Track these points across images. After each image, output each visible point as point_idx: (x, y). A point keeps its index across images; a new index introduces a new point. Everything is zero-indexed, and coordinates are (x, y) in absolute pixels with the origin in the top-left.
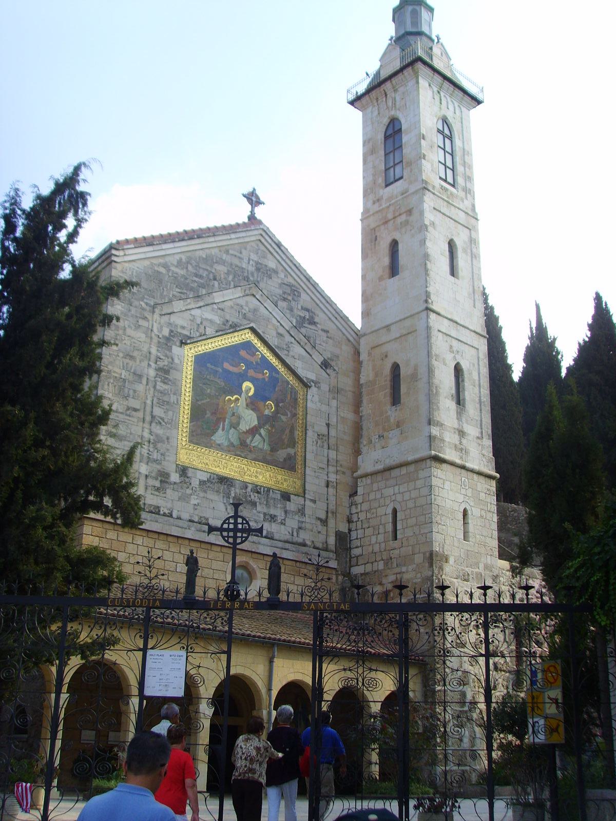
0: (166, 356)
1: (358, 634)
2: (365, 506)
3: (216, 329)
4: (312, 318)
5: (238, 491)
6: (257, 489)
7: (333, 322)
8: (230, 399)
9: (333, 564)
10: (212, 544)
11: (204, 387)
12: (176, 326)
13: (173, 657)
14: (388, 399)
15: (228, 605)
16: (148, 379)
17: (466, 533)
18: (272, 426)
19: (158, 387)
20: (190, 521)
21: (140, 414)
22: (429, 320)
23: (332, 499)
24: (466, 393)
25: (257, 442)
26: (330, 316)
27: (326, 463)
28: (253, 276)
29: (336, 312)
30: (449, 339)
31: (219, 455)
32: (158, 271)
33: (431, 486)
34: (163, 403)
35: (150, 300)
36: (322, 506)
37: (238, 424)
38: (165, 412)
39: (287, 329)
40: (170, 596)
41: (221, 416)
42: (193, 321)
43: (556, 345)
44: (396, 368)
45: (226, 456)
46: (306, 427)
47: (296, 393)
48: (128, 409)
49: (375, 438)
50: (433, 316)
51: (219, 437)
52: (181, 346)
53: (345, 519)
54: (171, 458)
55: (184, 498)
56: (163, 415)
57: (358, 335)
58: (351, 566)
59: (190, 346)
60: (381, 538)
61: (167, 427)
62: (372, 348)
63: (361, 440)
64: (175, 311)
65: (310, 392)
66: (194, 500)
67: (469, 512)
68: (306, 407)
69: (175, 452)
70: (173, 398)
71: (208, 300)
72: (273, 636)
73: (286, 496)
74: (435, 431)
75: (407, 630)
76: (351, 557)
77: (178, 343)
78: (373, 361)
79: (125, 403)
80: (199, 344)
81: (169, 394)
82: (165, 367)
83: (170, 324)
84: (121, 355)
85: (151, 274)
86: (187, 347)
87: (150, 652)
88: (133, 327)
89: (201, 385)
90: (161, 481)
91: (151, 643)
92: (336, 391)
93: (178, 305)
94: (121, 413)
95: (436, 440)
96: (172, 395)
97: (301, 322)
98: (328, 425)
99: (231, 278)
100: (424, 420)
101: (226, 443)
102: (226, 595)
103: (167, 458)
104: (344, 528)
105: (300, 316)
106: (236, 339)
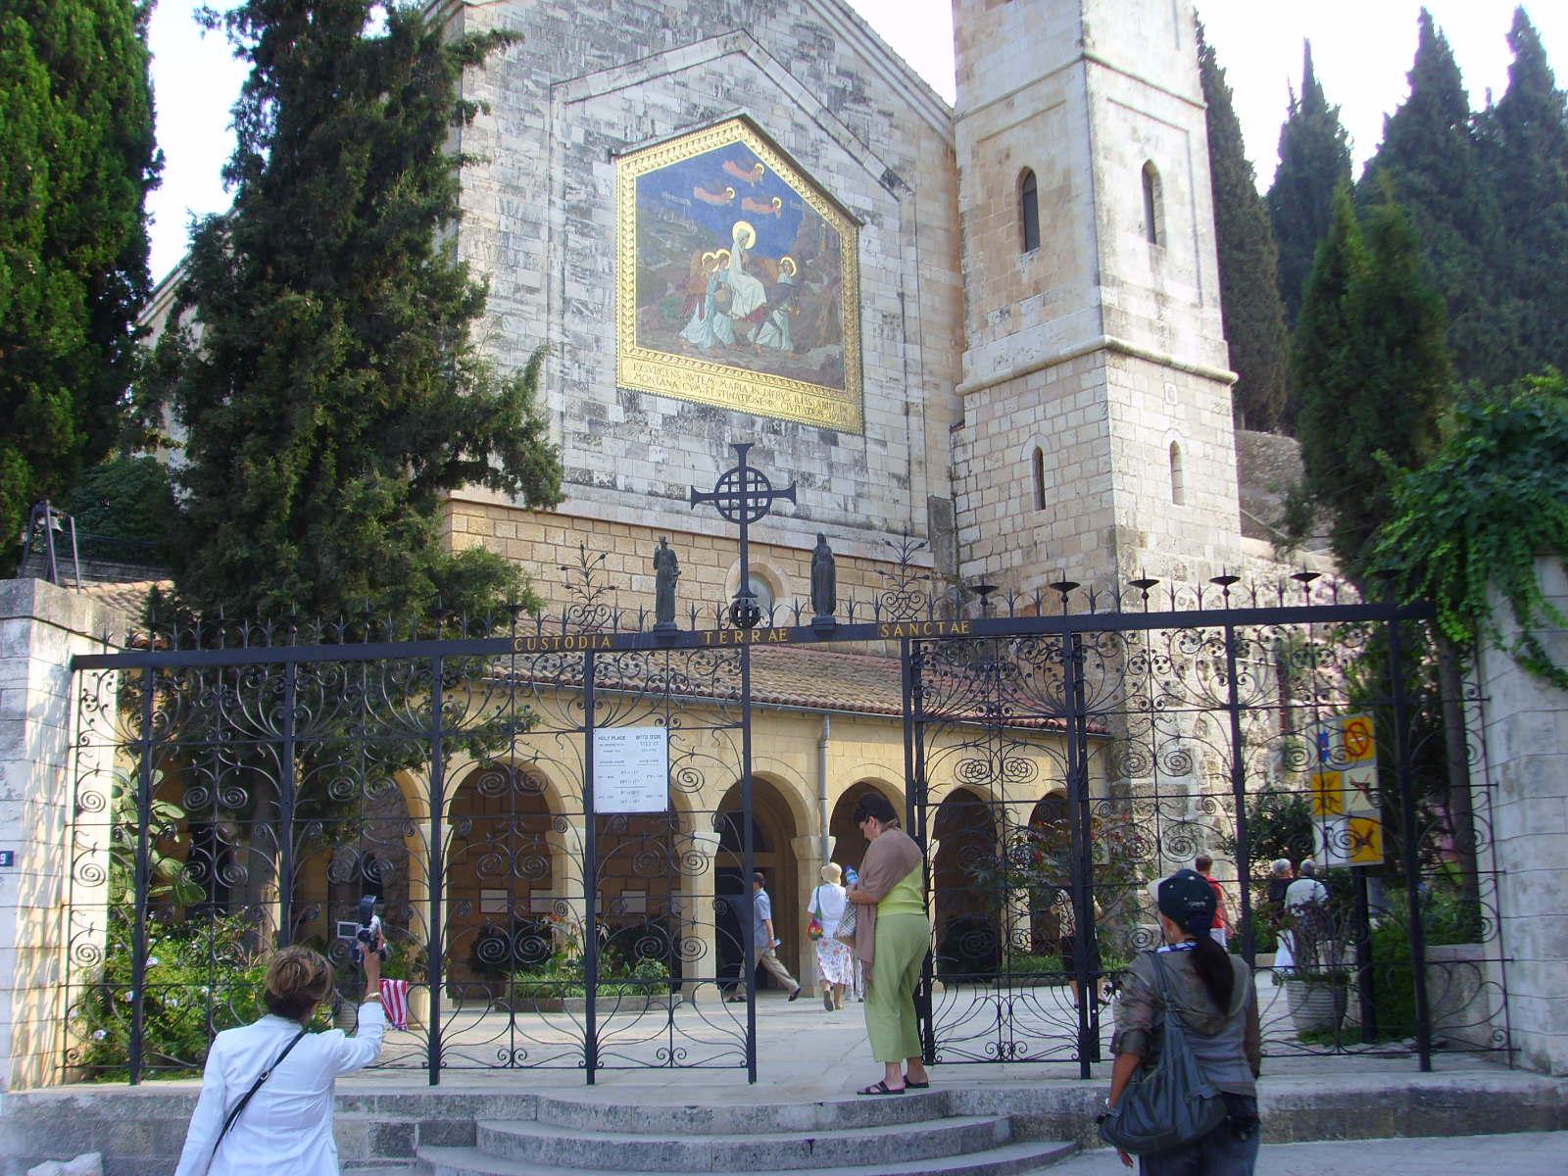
0: (582, 182)
1: (988, 677)
2: (981, 448)
3: (675, 123)
4: (860, 90)
5: (737, 431)
6: (773, 427)
7: (901, 96)
8: (712, 259)
9: (924, 559)
10: (694, 535)
11: (659, 237)
12: (597, 123)
13: (642, 740)
14: (1016, 239)
15: (739, 637)
16: (550, 229)
17: (1177, 489)
18: (795, 304)
19: (571, 244)
20: (651, 494)
21: (542, 298)
22: (1089, 80)
23: (917, 437)
24: (1168, 220)
25: (767, 336)
26: (895, 84)
28: (739, 15)
29: (906, 76)
30: (1130, 115)
32: (553, 18)
33: (1106, 402)
34: (582, 274)
35: (544, 76)
36: (898, 450)
37: (731, 304)
39: (812, 114)
40: (628, 621)
42: (628, 111)
43: (1340, 119)
44: (1027, 178)
47: (836, 238)
48: (518, 289)
49: (992, 317)
50: (1095, 71)
51: (695, 331)
53: (945, 474)
54: (607, 377)
55: (636, 452)
56: (584, 297)
57: (951, 118)
58: (959, 563)
59: (628, 159)
60: (1014, 506)
62: (981, 141)
63: (966, 322)
66: (655, 455)
67: (1182, 450)
70: (602, 263)
71: (655, 68)
72: (821, 700)
73: (829, 437)
74: (1108, 296)
75: (1079, 666)
76: (959, 546)
77: (603, 156)
78: (983, 166)
79: (512, 278)
80: (644, 154)
82: (582, 204)
83: (586, 120)
84: (496, 186)
85: (541, 24)
86: (621, 163)
87: (598, 733)
88: (515, 132)
90: (590, 423)
91: (598, 719)
92: (913, 230)
93: (597, 82)
94: (506, 298)
95: (1113, 315)
96: (599, 258)
97: (839, 98)
98: (901, 296)
99: (696, 20)
100: (1089, 278)
101: (709, 343)
102: (733, 619)
103: (598, 379)
104: (942, 490)
105: (836, 88)
106: (715, 140)
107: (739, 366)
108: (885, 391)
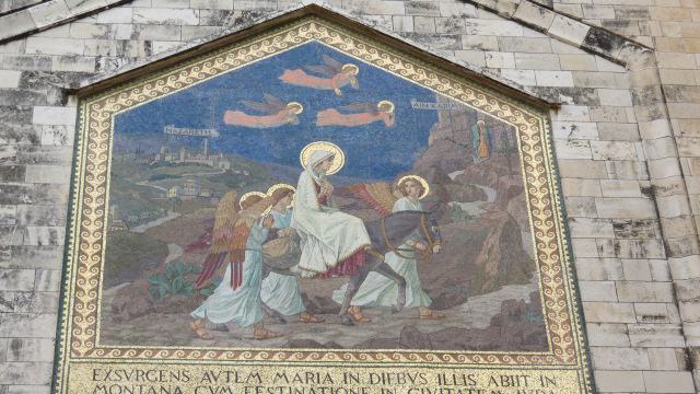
0: (12, 135)
8: (259, 199)
11: (156, 185)
12: (48, 60)
18: (430, 239)
25: (374, 288)
27: (669, 298)
31: (224, 356)
37: (296, 256)
38: (5, 276)
41: (225, 249)
42: (105, 37)
45: (255, 353)
46: (564, 211)
47: (508, 134)
51: (224, 304)
52: (64, 103)
61: (15, 315)
64: (39, 26)
65: (558, 120)
68: (555, 163)
69: (46, 376)
70: (36, 235)
77: (54, 97)
81: (24, 227)
82: (7, 164)
89: (143, 184)
96: (31, 229)
98: (650, 192)
101: (251, 320)
107: (313, 344)
108: (635, 339)
